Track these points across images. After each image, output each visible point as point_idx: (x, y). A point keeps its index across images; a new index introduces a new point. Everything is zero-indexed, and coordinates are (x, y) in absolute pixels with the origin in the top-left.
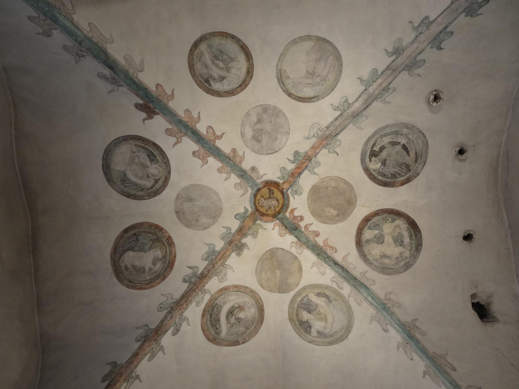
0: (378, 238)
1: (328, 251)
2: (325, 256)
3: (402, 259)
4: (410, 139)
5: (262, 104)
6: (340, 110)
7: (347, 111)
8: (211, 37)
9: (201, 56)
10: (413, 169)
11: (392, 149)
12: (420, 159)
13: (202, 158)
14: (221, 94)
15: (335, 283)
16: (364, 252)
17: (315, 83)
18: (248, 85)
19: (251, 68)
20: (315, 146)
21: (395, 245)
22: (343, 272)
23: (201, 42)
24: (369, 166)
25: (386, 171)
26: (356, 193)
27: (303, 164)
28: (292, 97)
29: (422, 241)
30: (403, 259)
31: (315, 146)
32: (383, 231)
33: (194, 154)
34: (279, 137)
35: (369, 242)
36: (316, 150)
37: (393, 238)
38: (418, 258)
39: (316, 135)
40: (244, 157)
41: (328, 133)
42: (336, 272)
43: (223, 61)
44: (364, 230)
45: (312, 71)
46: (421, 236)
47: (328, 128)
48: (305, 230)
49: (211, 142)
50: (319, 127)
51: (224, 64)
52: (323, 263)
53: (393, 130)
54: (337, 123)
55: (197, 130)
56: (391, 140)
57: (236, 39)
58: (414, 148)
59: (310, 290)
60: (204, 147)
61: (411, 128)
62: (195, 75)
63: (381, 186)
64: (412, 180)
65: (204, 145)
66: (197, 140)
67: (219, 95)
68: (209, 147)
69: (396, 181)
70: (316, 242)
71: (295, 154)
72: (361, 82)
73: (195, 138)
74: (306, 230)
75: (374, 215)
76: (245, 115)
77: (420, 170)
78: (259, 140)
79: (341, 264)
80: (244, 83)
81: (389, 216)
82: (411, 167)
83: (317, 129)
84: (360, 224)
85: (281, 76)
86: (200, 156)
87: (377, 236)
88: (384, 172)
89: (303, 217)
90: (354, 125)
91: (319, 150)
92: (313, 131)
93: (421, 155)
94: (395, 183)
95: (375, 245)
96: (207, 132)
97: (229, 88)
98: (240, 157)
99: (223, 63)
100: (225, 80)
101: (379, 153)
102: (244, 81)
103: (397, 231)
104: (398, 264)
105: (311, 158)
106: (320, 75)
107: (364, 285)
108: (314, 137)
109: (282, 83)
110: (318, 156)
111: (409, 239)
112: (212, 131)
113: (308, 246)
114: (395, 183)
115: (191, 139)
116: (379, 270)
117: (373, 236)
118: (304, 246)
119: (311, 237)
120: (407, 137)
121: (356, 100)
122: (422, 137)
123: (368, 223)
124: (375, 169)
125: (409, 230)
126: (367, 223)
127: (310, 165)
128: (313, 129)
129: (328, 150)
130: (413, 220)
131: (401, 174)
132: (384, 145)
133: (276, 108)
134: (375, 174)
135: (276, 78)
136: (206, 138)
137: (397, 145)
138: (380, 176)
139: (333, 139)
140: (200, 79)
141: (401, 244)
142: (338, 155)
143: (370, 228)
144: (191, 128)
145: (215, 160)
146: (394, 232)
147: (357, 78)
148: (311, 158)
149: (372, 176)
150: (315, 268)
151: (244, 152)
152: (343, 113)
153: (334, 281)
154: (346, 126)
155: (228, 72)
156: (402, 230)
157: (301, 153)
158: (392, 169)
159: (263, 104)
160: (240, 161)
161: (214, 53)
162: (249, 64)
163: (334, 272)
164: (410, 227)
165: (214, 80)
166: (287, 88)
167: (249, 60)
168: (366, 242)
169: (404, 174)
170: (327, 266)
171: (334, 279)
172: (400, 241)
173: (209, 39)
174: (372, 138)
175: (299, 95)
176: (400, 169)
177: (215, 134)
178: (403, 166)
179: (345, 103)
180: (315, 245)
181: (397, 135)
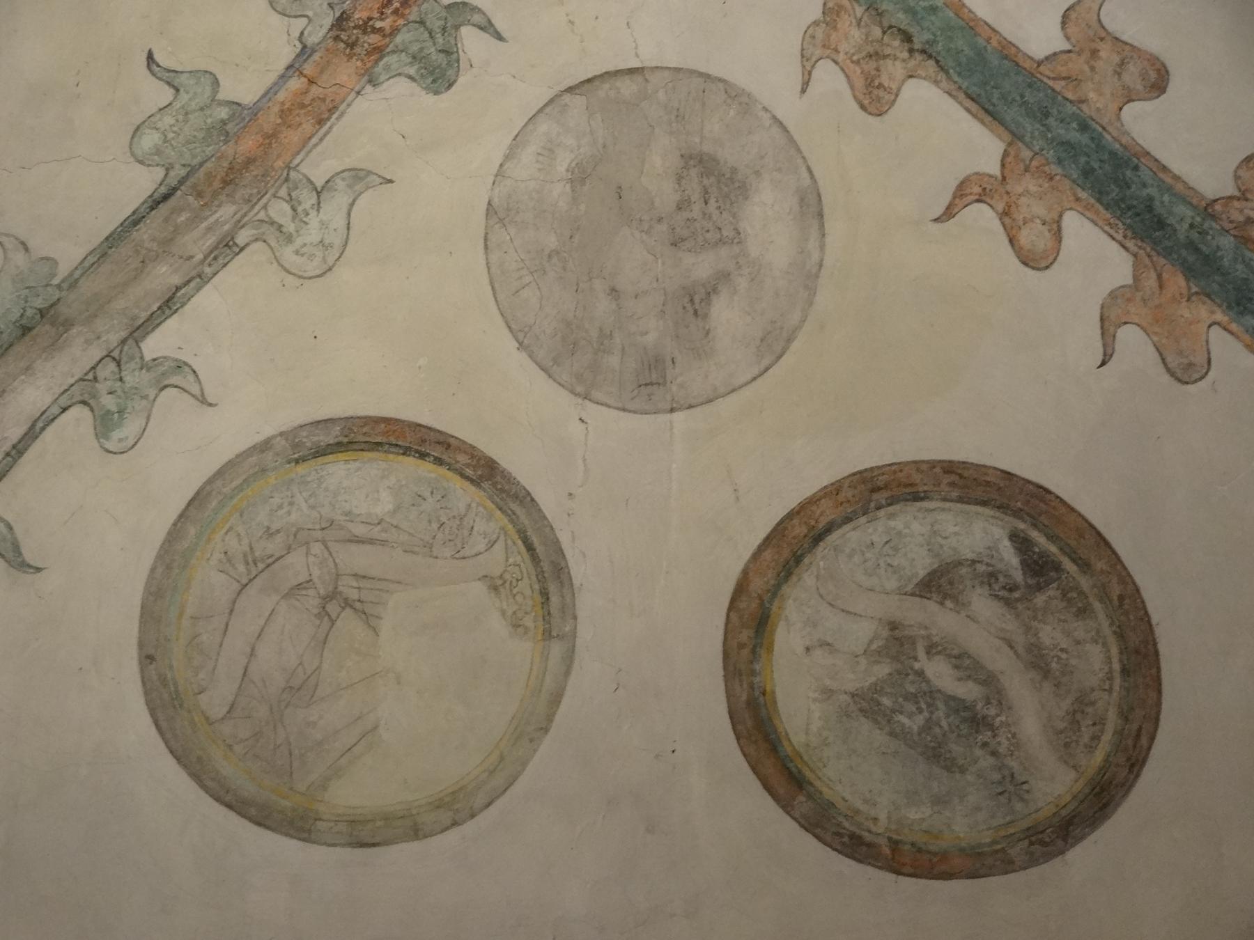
5: (675, 415)
6: (144, 366)
7: (96, 353)
8: (999, 847)
9: (1075, 724)
13: (1105, 51)
14: (952, 484)
17: (317, 548)
18: (767, 541)
19: (745, 652)
20: (308, 127)
23: (1064, 813)
28: (473, 457)
31: (308, 127)
33: (1153, 75)
34: (559, 192)
39: (308, 199)
40: (803, 56)
41: (226, 212)
43: (932, 694)
45: (339, 623)
47: (227, 247)
49: (1035, 163)
50: (288, 254)
51: (920, 674)
54: (164, 275)
55: (1130, 244)
57: (838, 834)
60: (1084, 127)
62: (1121, 606)
65: (1084, 139)
66: (1129, 173)
67: (961, 476)
68: (1051, 121)
71: (450, 72)
72: (16, 548)
73: (1144, 185)
76: (789, 341)
78: (694, 172)
80: (794, 554)
83: (299, 242)
85: (545, 594)
86: (1116, 59)
90: (48, 259)
91: (281, 96)
92: (323, 225)
96: (1059, 229)
97: (897, 524)
98: (831, 52)
99: (928, 682)
100: (922, 574)
102: (789, 568)
105: (337, 38)
106: (286, 596)
108: (319, 183)
109: (540, 549)
110: (287, 53)
112: (1026, 237)
115: (1177, 178)
121: (43, 429)
128: (327, 242)
129: (220, 96)
133: (579, 389)
135: (576, 582)
136: (1067, 182)
139: (183, 172)
140: (1085, 583)
142: (150, 57)
144: (1167, 253)
145: (1008, 30)
147: (38, 570)
151: (803, 91)
152: (124, 342)
154: (104, 255)
155: (893, 626)
157: (411, 78)
159: (664, 418)
160: (835, 28)
161: (985, 745)
162: (753, 673)
165: (993, 576)
166: (504, 521)
167: (752, 704)
173: (1012, 831)
175: (426, 469)
177: (1005, 214)
179: (114, 409)
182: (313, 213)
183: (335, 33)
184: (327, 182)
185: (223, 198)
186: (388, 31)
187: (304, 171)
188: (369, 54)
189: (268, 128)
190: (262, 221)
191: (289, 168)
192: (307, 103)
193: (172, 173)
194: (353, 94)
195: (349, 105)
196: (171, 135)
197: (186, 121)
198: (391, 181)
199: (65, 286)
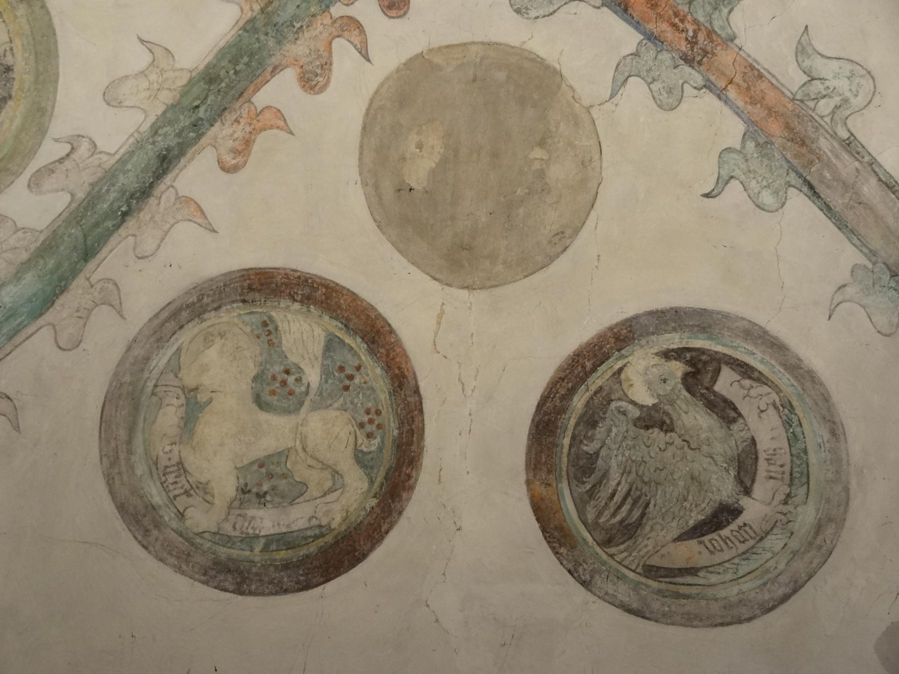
0: (284, 383)
1: (227, 130)
2: (202, 109)
3: (177, 492)
4: (762, 539)
10: (612, 556)
11: (719, 459)
12: (659, 592)
15: (63, 154)
16: (216, 309)
21: (246, 462)
22: (123, 192)
24: (642, 347)
25: (614, 430)
26: (508, 289)
27: (674, 25)
29: (263, 594)
30: (175, 497)
31: (763, 85)
32: (315, 407)
35: (264, 338)
36: (739, 86)
37: (280, 454)
38: (179, 570)
39: (817, 86)
41: (824, 144)
42: (123, 161)
44: (326, 318)
46: (286, 591)
47: (850, 144)
48: (334, 22)
52: (167, 97)
53: (813, 458)
56: (765, 451)
58: (718, 558)
59: (27, 27)
61: (818, 541)
63: (540, 406)
64: (556, 553)
69: (558, 479)
70: (276, 70)
74: (337, 25)
75: (397, 371)
77: (606, 594)
79: (162, 187)
81: (389, 443)
82: (622, 547)
83: (848, 94)
84: (354, 296)
87: (291, 379)
88: (608, 422)
89: (402, 12)
90: (852, 271)
91: (740, 104)
92: (836, 76)
93: (678, 596)
94: (549, 472)
95: (251, 365)
101: (702, 395)
103: (316, 479)
104: (155, 474)
107: (57, 296)
108: (806, 78)
110: (709, 99)
111: (272, 531)
113: (255, 30)
114: (549, 472)
116: (127, 378)
117: (293, 359)
118: (257, 7)
119: (299, 49)
120: (772, 529)
122: (767, 596)
123: (359, 340)
124: (623, 376)
125: (316, 537)
126: (356, 332)
127: (665, 56)
128: (848, 74)
129: (738, 147)
130: (364, 556)
131: (592, 503)
132: (741, 421)
134: (597, 381)
137: (739, 480)
138: (588, 402)
139: (793, 175)
141: (249, 491)
142: (707, 195)
143: (331, 344)
146: (313, 463)
148: (700, 63)
149: (589, 365)
150: (143, 59)
153: (73, 149)
154: (852, 231)
156: (318, 501)
157: (730, 12)
158: (620, 458)
163: (122, 151)
164: (329, 539)
168: (265, 324)
169: (590, 516)
170: (152, 118)
171: (84, 148)
172: (265, 488)
174: (781, 364)
176: (618, 498)
178: (630, 511)
180: (261, 63)
181: (787, 477)
182: (827, 83)
183: (696, 64)
184: (805, 73)
185: (814, 146)
186: (696, 27)
187: (796, 89)
188: (712, 41)
189: (763, 114)
190: (832, 120)
191: (793, 99)
192: (745, 85)
193: (793, 183)
194: (741, 53)
195: (749, 56)
196: (765, 183)
197: (755, 172)
198: (806, 27)
199: (874, 259)
